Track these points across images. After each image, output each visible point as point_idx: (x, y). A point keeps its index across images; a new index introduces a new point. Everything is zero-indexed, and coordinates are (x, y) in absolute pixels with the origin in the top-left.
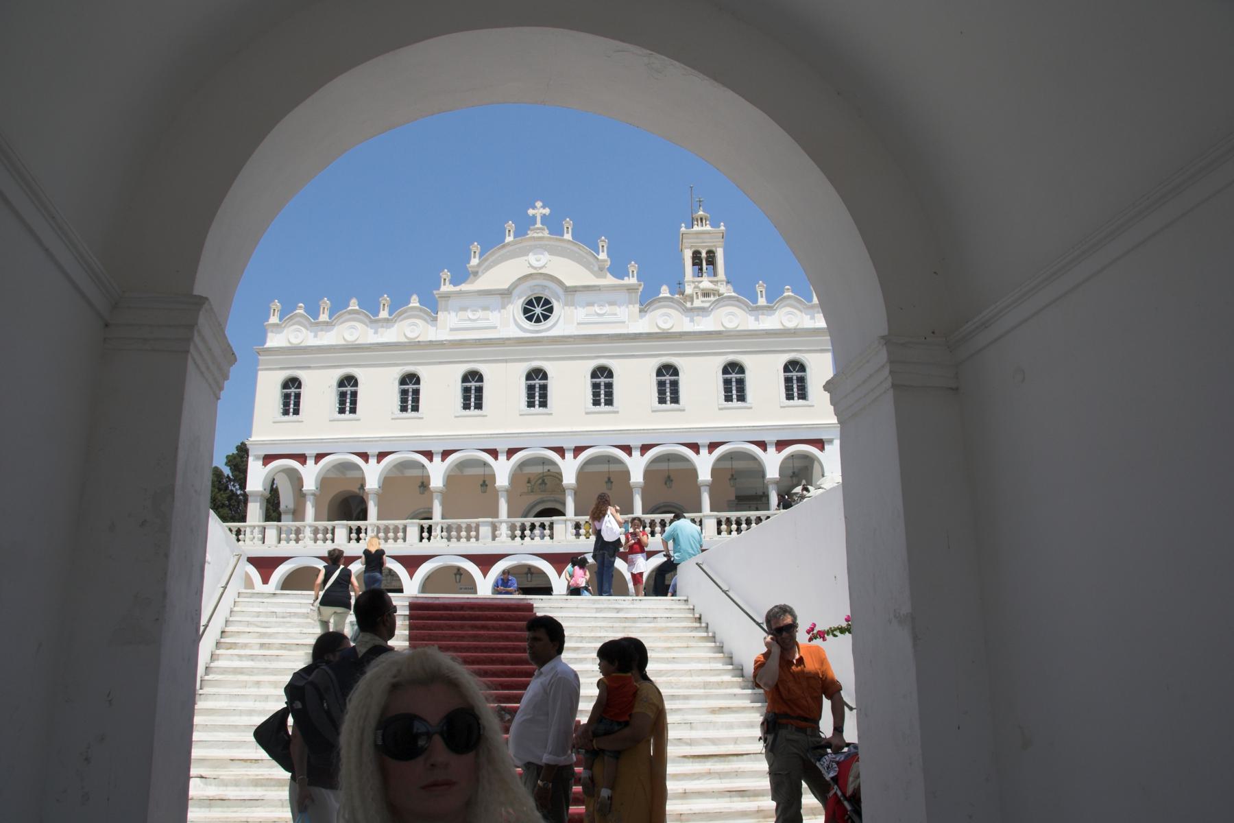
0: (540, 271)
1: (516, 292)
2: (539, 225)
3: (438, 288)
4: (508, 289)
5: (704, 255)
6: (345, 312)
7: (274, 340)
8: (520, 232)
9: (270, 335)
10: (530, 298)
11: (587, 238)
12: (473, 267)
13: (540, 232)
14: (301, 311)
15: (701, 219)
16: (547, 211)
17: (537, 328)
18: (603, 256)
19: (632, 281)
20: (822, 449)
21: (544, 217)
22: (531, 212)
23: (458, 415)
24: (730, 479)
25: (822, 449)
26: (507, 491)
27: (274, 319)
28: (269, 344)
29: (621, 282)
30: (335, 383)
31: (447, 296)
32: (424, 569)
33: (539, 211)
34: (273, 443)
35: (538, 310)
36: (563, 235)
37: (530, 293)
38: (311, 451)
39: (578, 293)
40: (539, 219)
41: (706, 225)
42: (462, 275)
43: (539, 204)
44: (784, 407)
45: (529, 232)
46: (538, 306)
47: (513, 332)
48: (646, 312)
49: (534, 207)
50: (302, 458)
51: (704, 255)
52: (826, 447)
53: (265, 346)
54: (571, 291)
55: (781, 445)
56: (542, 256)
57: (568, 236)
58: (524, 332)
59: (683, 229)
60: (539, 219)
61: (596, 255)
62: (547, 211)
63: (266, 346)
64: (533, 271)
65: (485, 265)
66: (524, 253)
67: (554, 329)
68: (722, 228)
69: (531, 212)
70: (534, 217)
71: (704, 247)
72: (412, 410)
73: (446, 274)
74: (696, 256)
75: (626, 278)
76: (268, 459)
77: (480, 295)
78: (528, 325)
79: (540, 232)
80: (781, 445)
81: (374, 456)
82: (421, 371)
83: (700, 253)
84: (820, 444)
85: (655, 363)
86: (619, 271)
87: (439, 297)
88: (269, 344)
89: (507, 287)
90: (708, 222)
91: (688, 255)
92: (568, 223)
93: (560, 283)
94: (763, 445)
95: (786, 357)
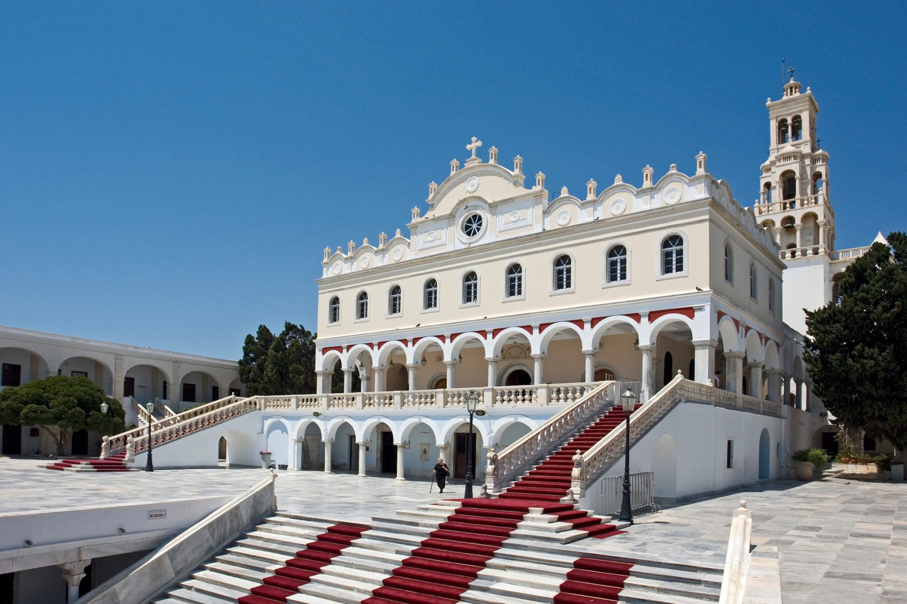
0: (474, 194)
1: (457, 215)
3: (410, 222)
4: (451, 214)
5: (789, 121)
7: (327, 274)
9: (325, 269)
10: (469, 217)
11: (506, 161)
15: (791, 88)
18: (517, 172)
19: (537, 188)
27: (325, 260)
28: (324, 276)
30: (355, 298)
31: (415, 226)
35: (474, 226)
40: (473, 152)
41: (796, 92)
42: (425, 208)
45: (465, 164)
46: (472, 224)
48: (549, 213)
51: (789, 121)
53: (322, 278)
54: (494, 207)
60: (473, 152)
63: (322, 278)
64: (470, 195)
65: (439, 196)
68: (809, 92)
73: (416, 210)
74: (782, 123)
75: (534, 187)
78: (465, 238)
83: (786, 121)
85: (552, 256)
86: (529, 184)
88: (324, 276)
89: (449, 212)
90: (797, 90)
91: (773, 125)
93: (485, 201)
95: (663, 234)
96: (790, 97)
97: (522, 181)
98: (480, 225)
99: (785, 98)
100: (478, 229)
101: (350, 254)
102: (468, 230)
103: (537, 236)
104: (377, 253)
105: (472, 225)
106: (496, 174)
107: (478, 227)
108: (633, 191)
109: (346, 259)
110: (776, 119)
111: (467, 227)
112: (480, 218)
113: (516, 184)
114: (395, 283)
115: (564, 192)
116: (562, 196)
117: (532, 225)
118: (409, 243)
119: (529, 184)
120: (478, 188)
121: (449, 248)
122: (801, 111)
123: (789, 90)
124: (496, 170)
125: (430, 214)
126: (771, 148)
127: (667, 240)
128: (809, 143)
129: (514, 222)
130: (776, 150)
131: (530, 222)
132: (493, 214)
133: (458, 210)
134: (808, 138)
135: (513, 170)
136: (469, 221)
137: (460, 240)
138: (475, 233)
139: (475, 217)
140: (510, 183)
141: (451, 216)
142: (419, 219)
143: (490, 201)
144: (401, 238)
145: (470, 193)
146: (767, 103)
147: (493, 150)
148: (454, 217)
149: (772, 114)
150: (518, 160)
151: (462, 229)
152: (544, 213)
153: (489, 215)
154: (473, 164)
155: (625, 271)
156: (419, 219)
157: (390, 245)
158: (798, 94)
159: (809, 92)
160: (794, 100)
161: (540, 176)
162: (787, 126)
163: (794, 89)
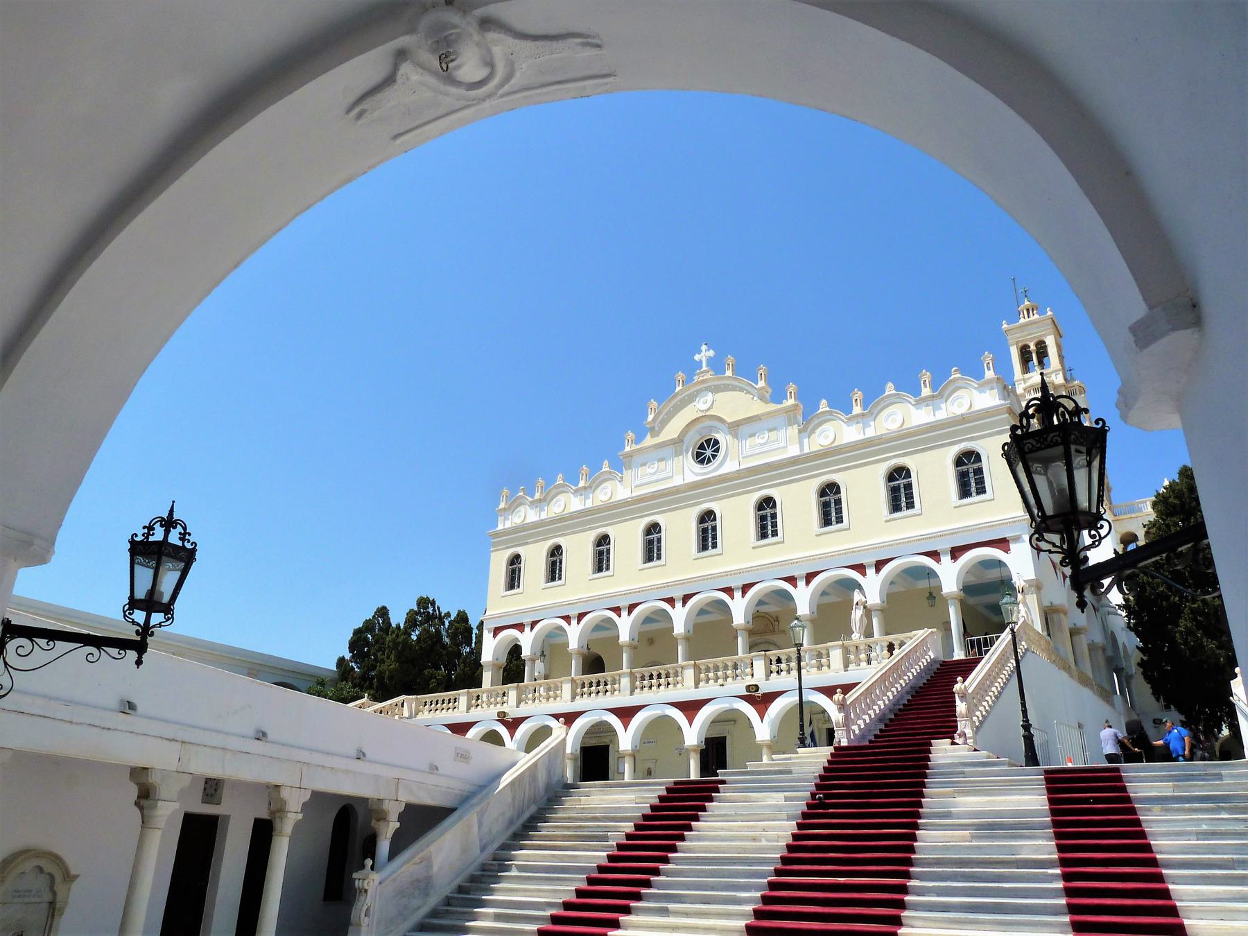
0: (707, 413)
1: (686, 439)
2: (704, 368)
5: (1033, 347)
6: (553, 488)
8: (688, 381)
9: (500, 519)
11: (746, 371)
12: (649, 423)
13: (705, 374)
14: (521, 494)
15: (1028, 310)
16: (711, 353)
17: (706, 470)
18: (761, 384)
19: (791, 402)
20: (1007, 550)
21: (709, 360)
22: (697, 357)
23: (641, 568)
24: (928, 598)
25: (1007, 550)
27: (502, 505)
29: (779, 406)
31: (630, 455)
33: (704, 354)
34: (500, 616)
35: (709, 452)
36: (725, 374)
37: (698, 437)
38: (527, 620)
39: (741, 427)
43: (704, 347)
47: (691, 478)
49: (700, 352)
50: (520, 627)
51: (1033, 347)
52: (1012, 546)
54: (735, 428)
56: (706, 398)
57: (729, 373)
58: (697, 476)
59: (1005, 326)
61: (755, 385)
62: (711, 353)
63: (497, 529)
66: (691, 399)
67: (724, 467)
68: (1049, 313)
69: (697, 357)
70: (701, 362)
71: (1031, 340)
76: (497, 631)
77: (657, 449)
78: (698, 468)
79: (705, 374)
80: (956, 553)
81: (575, 618)
82: (610, 531)
84: (1002, 543)
86: (778, 397)
87: (624, 458)
88: (500, 527)
90: (1035, 312)
91: (1015, 353)
92: (730, 359)
94: (934, 555)
95: (954, 450)
96: (1027, 319)
97: (768, 396)
98: (717, 450)
99: (1022, 321)
100: (714, 457)
101: (537, 496)
102: (701, 458)
103: (794, 461)
104: (576, 492)
105: (706, 451)
106: (734, 388)
107: (714, 453)
108: (911, 400)
109: (531, 502)
110: (1017, 344)
111: (699, 455)
112: (716, 442)
113: (762, 398)
114: (603, 530)
115: (824, 406)
116: (820, 410)
117: (787, 447)
118: (622, 478)
119: (778, 397)
120: (712, 405)
121: (677, 481)
122: (1045, 335)
123: (1025, 312)
124: (736, 383)
125: (649, 441)
126: (1016, 379)
127: (960, 456)
128: (1061, 372)
129: (761, 444)
130: (1023, 382)
131: (782, 444)
132: (736, 436)
133: (687, 432)
134: (1059, 366)
135: (757, 384)
136: (702, 447)
137: (691, 470)
138: (709, 461)
139: (708, 441)
140: (755, 398)
141: (678, 442)
142: (635, 447)
143: (729, 421)
144: (610, 473)
145: (702, 411)
146: (1003, 327)
147: (730, 359)
148: (682, 441)
149: (1012, 338)
150: (763, 369)
151: (693, 458)
152: (800, 432)
153: (729, 437)
154: (705, 377)
155: (912, 498)
156: (635, 447)
157: (593, 482)
158: (1036, 316)
159: (1049, 313)
160: (1034, 322)
161: (792, 388)
162: (1030, 353)
163: (1031, 312)
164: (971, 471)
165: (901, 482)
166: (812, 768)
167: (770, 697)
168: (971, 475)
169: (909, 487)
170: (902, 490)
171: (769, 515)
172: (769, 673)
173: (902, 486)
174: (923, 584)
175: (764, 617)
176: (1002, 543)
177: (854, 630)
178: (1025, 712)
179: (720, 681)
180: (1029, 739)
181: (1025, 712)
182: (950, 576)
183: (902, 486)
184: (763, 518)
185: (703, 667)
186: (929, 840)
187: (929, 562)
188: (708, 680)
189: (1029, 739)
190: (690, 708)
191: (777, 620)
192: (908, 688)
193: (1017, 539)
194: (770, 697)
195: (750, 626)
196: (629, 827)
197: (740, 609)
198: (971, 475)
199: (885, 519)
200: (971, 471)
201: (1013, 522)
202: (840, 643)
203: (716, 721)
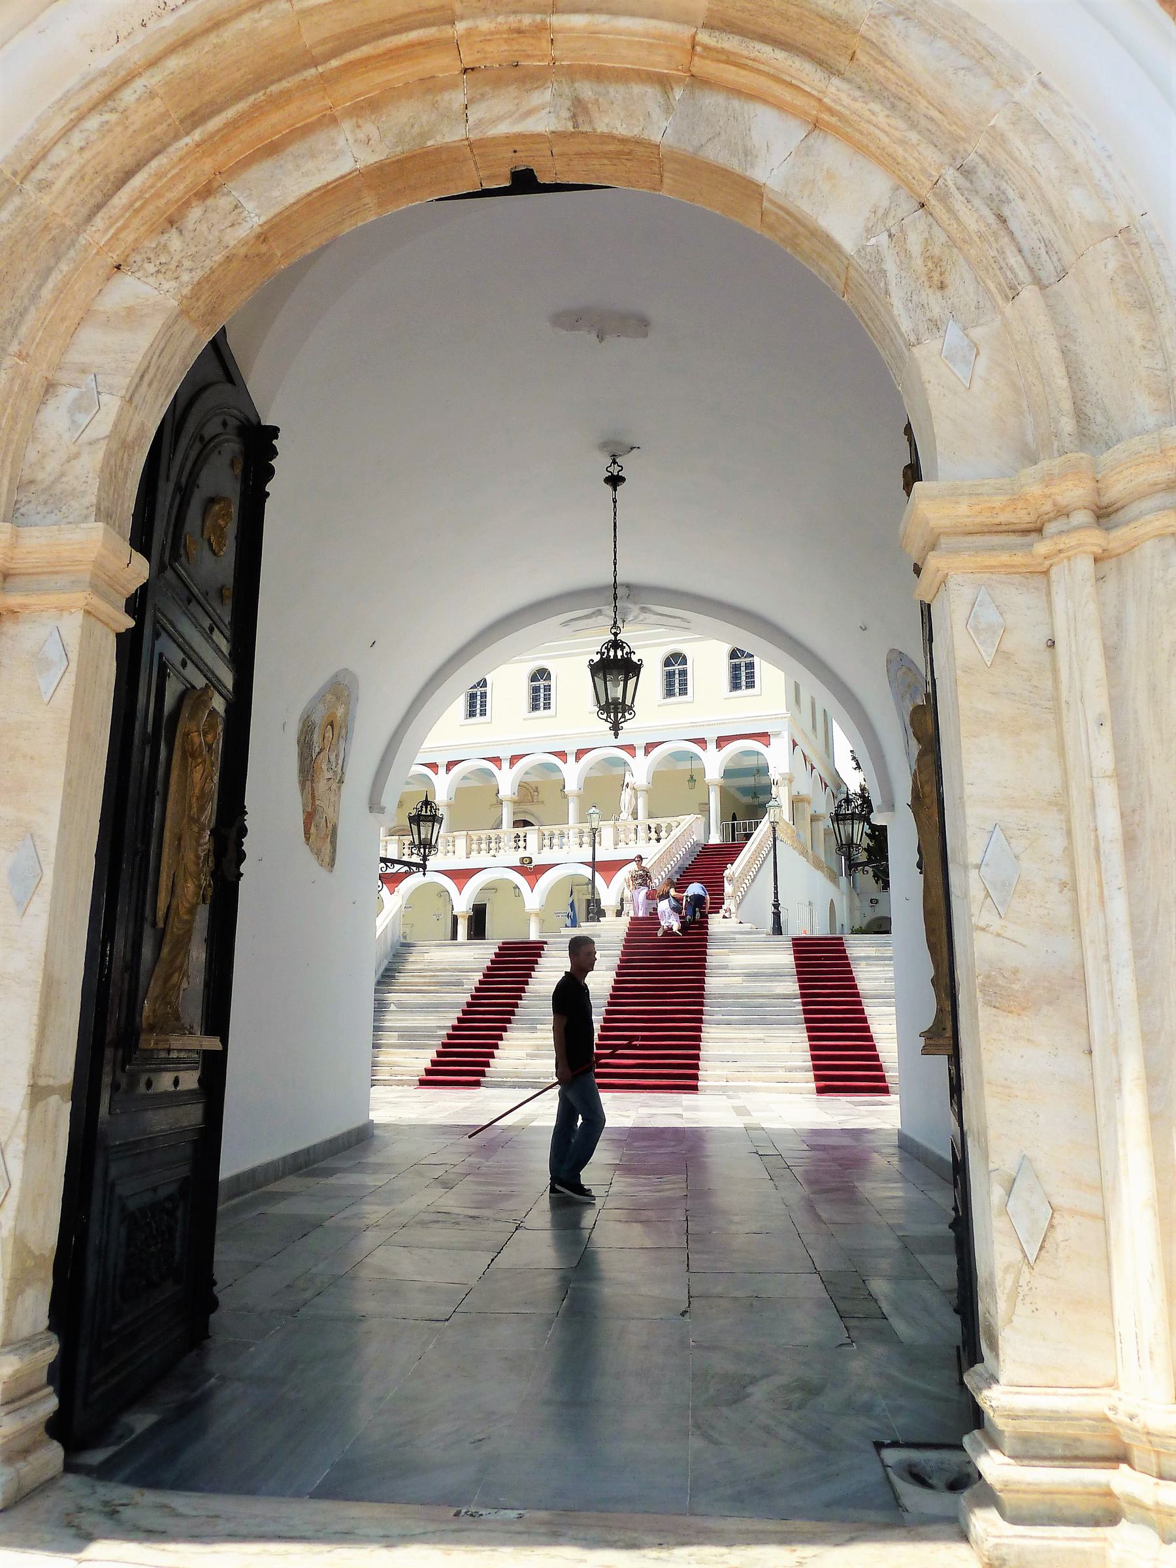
20: (767, 745)
25: (767, 745)
26: (578, 796)
32: (546, 880)
44: (463, 725)
52: (772, 740)
55: (722, 742)
72: (544, 708)
80: (722, 742)
84: (763, 737)
94: (701, 742)
164: (743, 664)
165: (677, 668)
166: (617, 934)
167: (542, 869)
168: (743, 669)
169: (683, 673)
170: (677, 676)
171: (542, 686)
172: (542, 847)
173: (677, 672)
174: (686, 765)
175: (524, 787)
176: (763, 737)
177: (623, 809)
178: (776, 894)
179: (492, 852)
180: (777, 916)
181: (776, 894)
182: (714, 763)
183: (677, 672)
184: (536, 690)
185: (475, 838)
186: (712, 983)
187: (695, 748)
188: (479, 851)
189: (777, 916)
190: (461, 876)
191: (537, 790)
192: (676, 869)
193: (778, 734)
194: (542, 869)
195: (516, 798)
196: (479, 976)
197: (507, 781)
198: (743, 669)
199: (659, 703)
200: (743, 664)
201: (776, 717)
202: (612, 822)
203: (487, 889)
